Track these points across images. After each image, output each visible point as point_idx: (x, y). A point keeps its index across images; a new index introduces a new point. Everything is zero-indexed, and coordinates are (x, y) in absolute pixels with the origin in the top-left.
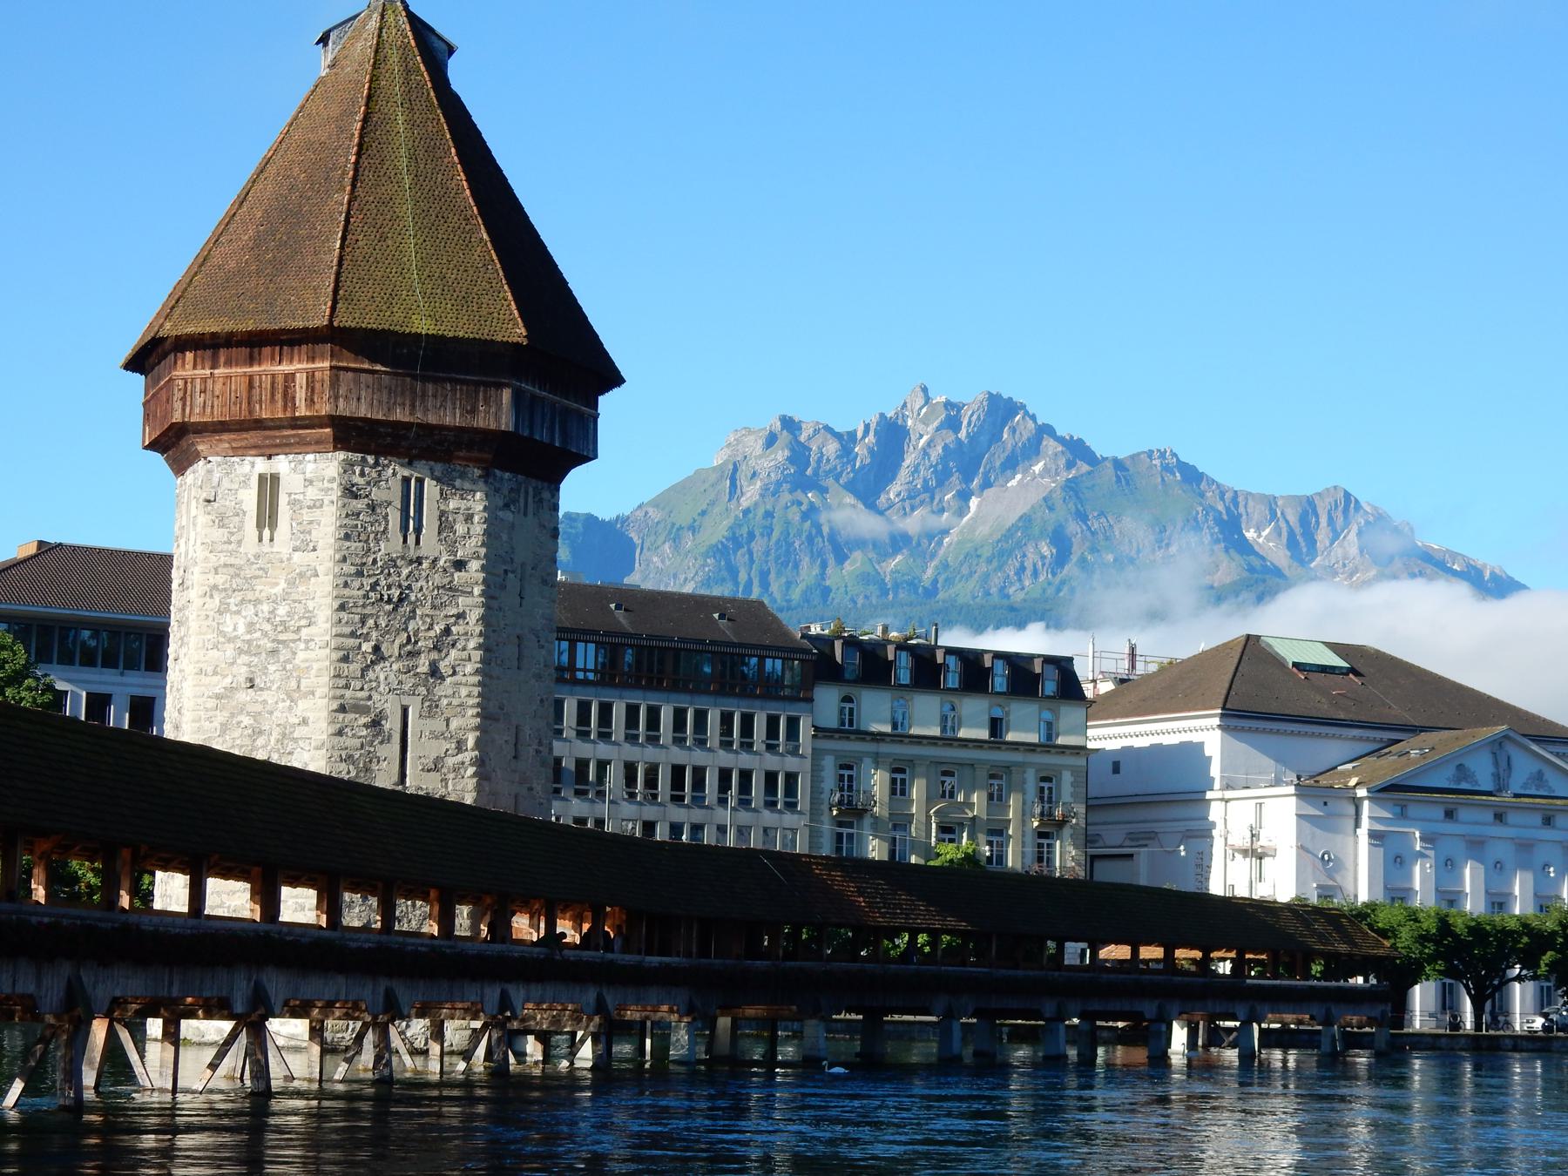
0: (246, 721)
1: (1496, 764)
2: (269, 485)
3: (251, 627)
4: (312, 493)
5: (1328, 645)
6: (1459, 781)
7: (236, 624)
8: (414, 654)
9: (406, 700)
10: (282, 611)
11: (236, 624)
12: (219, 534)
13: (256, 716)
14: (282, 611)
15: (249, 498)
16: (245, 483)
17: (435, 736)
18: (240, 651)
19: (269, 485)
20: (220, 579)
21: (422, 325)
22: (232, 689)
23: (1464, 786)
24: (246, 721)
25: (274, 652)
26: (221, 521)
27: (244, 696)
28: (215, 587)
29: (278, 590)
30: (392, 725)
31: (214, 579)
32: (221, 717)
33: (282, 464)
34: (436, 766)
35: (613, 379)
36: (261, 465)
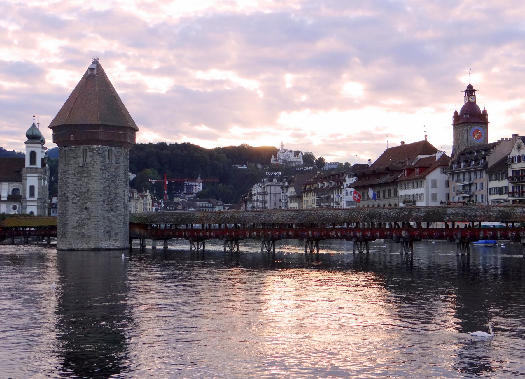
0: (108, 192)
2: (110, 151)
3: (108, 176)
4: (118, 154)
7: (106, 175)
10: (114, 174)
11: (106, 175)
12: (102, 159)
13: (110, 192)
14: (114, 174)
15: (107, 153)
16: (106, 151)
18: (107, 180)
19: (110, 151)
20: (103, 167)
22: (105, 187)
24: (108, 192)
25: (113, 181)
26: (102, 157)
27: (107, 188)
28: (101, 169)
29: (113, 170)
31: (101, 167)
32: (103, 192)
33: (113, 148)
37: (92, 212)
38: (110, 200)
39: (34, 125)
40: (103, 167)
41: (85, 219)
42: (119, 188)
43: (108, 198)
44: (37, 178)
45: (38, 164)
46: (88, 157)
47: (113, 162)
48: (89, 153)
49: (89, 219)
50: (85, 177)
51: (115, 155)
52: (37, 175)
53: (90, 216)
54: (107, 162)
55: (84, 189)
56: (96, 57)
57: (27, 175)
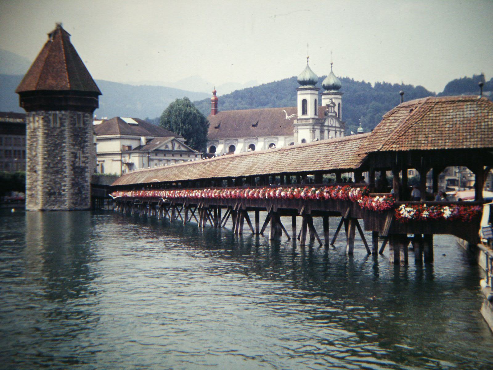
1: (172, 145)
5: (133, 119)
6: (166, 148)
8: (80, 144)
9: (79, 152)
17: (84, 157)
19: (55, 115)
21: (82, 89)
23: (167, 149)
30: (78, 155)
33: (58, 112)
34: (83, 162)
35: (101, 94)
36: (53, 112)
37: (39, 175)
38: (54, 163)
39: (308, 67)
40: (46, 131)
41: (34, 181)
42: (65, 151)
43: (53, 161)
44: (308, 130)
45: (311, 113)
46: (36, 121)
47: (58, 125)
48: (37, 119)
49: (37, 181)
50: (34, 141)
51: (60, 119)
52: (308, 127)
53: (37, 178)
54: (52, 125)
55: (34, 153)
56: (59, 21)
57: (299, 127)
